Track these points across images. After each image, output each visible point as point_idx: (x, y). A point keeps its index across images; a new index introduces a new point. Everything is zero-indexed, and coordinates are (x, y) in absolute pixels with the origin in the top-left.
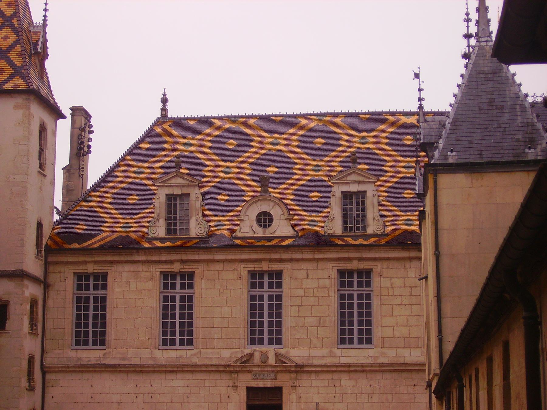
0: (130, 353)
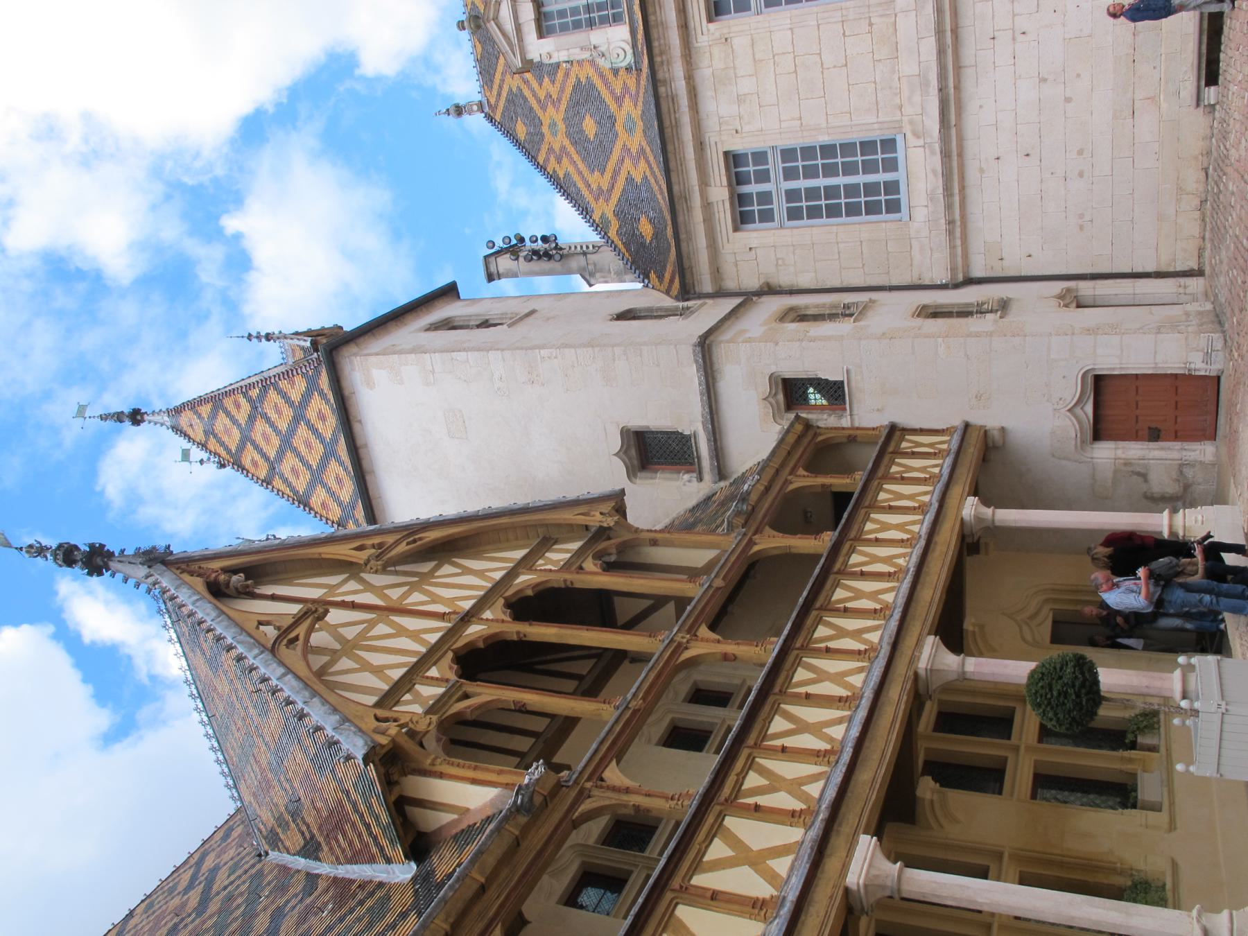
0: (908, 67)
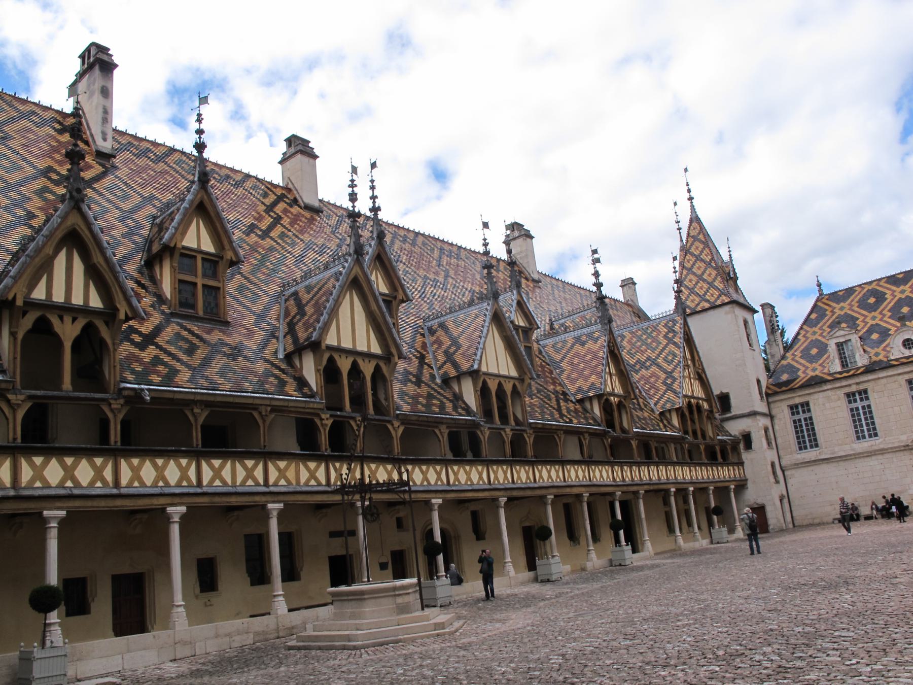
0: (836, 449)
